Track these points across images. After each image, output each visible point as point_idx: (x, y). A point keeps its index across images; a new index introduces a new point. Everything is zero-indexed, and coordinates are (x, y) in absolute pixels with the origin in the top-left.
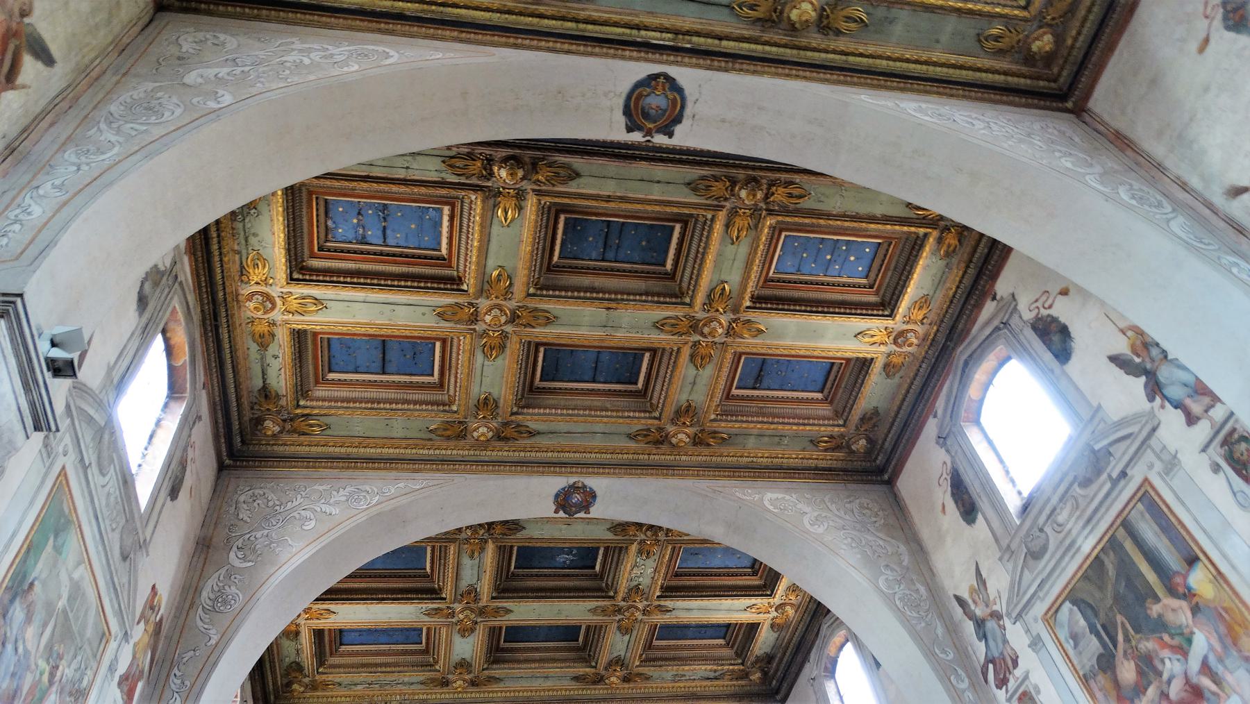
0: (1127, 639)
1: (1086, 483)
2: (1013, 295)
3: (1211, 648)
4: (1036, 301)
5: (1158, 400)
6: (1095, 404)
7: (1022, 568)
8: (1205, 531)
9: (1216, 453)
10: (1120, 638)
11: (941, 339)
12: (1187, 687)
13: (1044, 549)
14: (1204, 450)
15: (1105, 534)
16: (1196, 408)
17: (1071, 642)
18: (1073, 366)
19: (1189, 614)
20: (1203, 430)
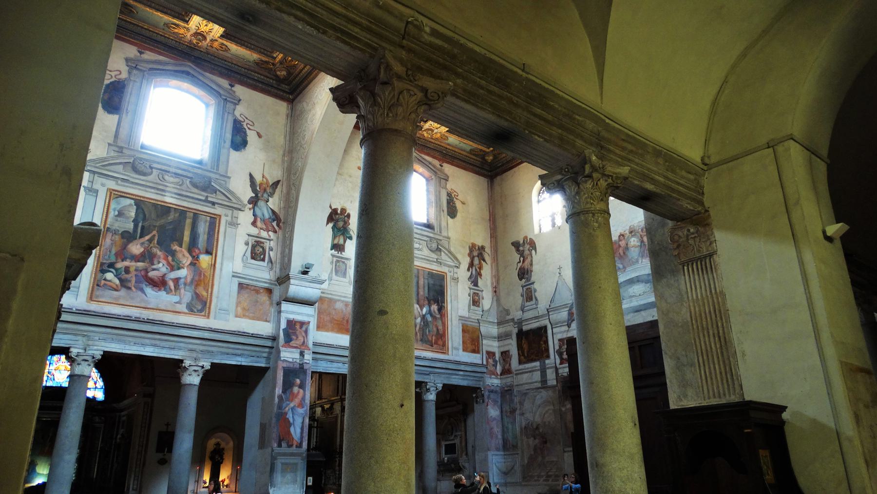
0: (150, 241)
1: (195, 185)
2: (240, 100)
3: (186, 278)
4: (247, 118)
5: (251, 206)
6: (229, 175)
7: (120, 163)
8: (223, 251)
9: (251, 241)
10: (147, 238)
11: (196, 54)
12: (161, 278)
13: (144, 174)
14: (248, 235)
15: (184, 207)
16: (259, 224)
17: (117, 213)
18: (234, 154)
19: (189, 262)
20: (254, 231)
